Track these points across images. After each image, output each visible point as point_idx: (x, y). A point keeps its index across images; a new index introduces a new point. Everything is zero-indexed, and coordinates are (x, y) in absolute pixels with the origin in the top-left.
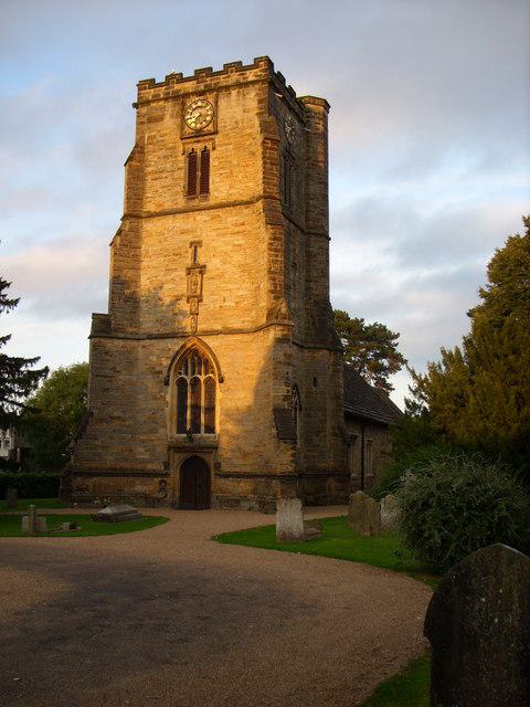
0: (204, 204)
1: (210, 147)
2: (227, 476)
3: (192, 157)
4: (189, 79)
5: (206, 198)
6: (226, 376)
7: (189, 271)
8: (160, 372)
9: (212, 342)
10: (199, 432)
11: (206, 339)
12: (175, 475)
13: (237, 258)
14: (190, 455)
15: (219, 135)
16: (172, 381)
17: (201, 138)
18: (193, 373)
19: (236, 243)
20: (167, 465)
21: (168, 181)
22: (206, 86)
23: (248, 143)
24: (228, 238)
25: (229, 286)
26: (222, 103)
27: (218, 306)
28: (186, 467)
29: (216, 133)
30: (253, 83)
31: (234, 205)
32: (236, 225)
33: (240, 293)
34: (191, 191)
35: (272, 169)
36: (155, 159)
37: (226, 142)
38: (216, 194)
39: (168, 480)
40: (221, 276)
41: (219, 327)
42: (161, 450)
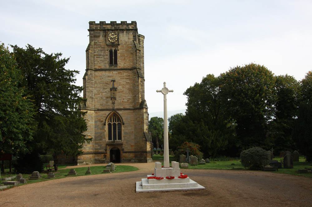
0: (116, 68)
1: (117, 49)
2: (126, 152)
3: (111, 52)
4: (108, 24)
5: (116, 66)
6: (125, 123)
7: (111, 90)
8: (102, 121)
9: (120, 112)
10: (116, 140)
11: (118, 111)
12: (108, 152)
13: (128, 86)
14: (113, 147)
15: (120, 46)
16: (107, 124)
17: (114, 46)
18: (113, 121)
19: (127, 82)
20: (106, 150)
21: (103, 59)
22: (115, 28)
23: (130, 49)
24: (125, 80)
25: (125, 95)
26: (121, 35)
27: (121, 101)
28: (112, 152)
29: (119, 45)
30: (132, 30)
32: (127, 76)
33: (129, 98)
34: (111, 63)
36: (97, 50)
37: (123, 48)
38: (120, 65)
39: (106, 155)
40: (123, 91)
41: (122, 108)
42: (104, 145)
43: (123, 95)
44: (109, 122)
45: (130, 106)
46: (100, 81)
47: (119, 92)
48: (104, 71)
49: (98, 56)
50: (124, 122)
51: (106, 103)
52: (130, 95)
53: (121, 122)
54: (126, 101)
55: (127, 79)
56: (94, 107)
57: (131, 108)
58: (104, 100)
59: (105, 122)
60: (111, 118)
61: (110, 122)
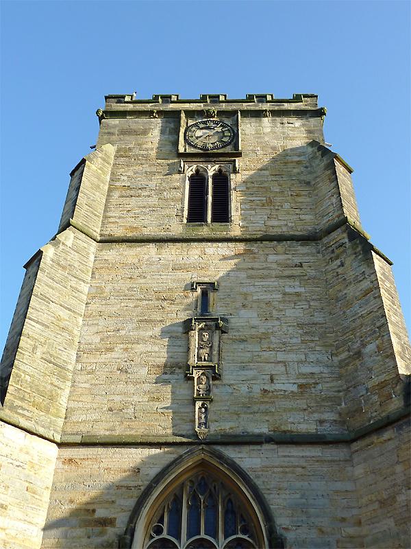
1: (226, 168)
8: (106, 522)
9: (247, 459)
11: (231, 453)
13: (294, 313)
19: (288, 290)
21: (154, 201)
23: (295, 171)
24: (272, 283)
27: (257, 389)
29: (239, 155)
31: (280, 239)
32: (287, 266)
33: (307, 369)
34: (196, 214)
40: (265, 336)
41: (264, 429)
43: (266, 354)
44: (159, 531)
45: (321, 422)
46: (124, 285)
47: (243, 341)
48: (152, 245)
49: (132, 193)
50: (279, 530)
51: (153, 399)
52: (312, 357)
53: (256, 534)
54: (295, 388)
55: (289, 277)
56: (60, 422)
57: (328, 430)
58: (136, 383)
59: (131, 531)
60: (177, 501)
61: (165, 535)
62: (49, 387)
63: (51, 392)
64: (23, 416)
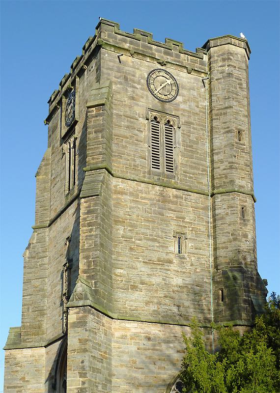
35: (97, 138)
62: (38, 323)
63: (39, 324)
64: (29, 342)
